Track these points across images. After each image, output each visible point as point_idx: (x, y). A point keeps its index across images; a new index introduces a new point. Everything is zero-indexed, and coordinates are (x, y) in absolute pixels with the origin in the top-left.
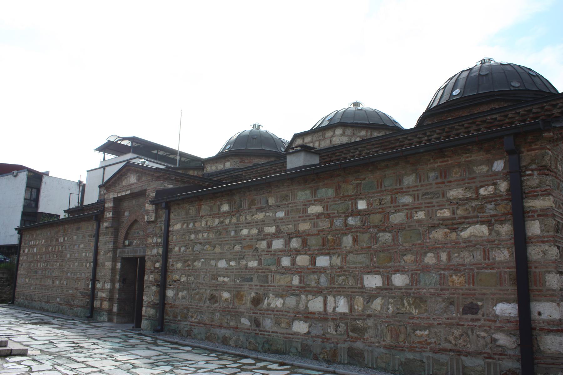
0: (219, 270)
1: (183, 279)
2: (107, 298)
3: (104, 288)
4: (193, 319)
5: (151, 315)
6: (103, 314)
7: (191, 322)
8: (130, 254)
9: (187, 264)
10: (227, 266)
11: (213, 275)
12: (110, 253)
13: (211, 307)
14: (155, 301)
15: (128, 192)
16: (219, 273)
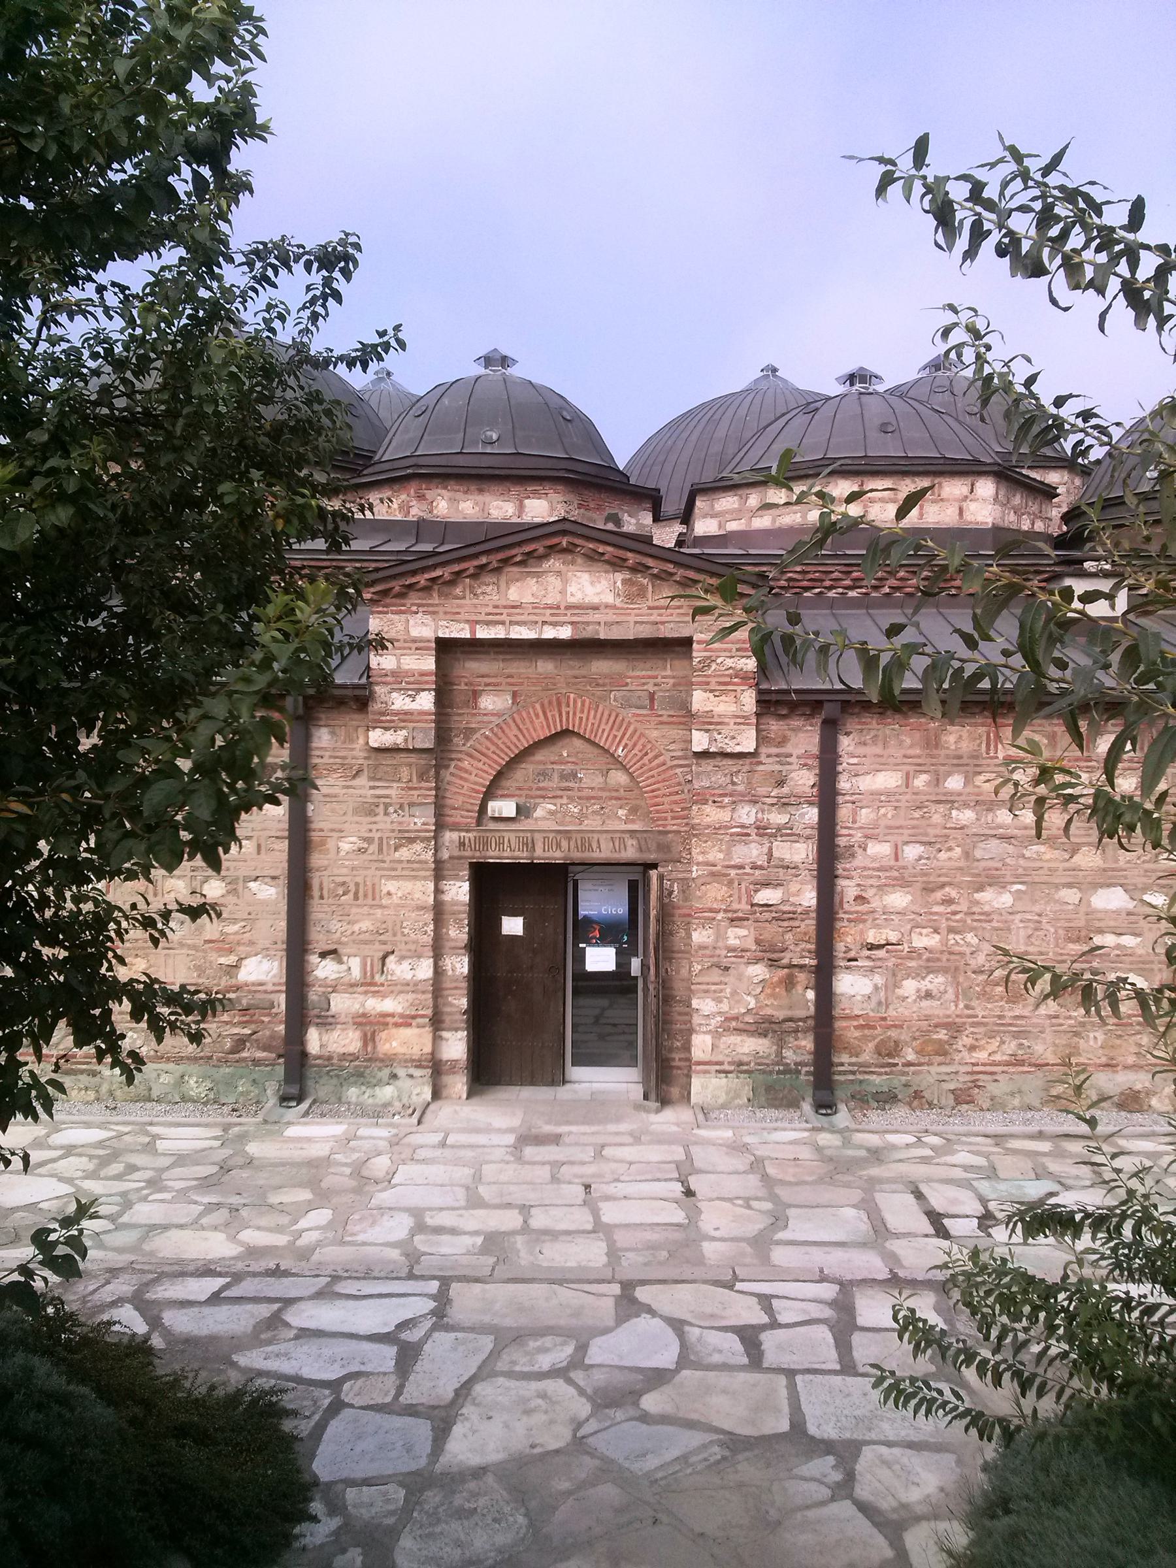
0: (1099, 916)
1: (924, 940)
2: (414, 1017)
3: (378, 978)
4: (981, 1056)
5: (745, 1059)
6: (394, 1076)
7: (974, 1064)
8: (539, 852)
9: (939, 895)
10: (1131, 905)
11: (1067, 929)
12: (418, 847)
13: (1070, 1017)
14: (769, 1011)
15: (565, 633)
16: (1098, 924)
